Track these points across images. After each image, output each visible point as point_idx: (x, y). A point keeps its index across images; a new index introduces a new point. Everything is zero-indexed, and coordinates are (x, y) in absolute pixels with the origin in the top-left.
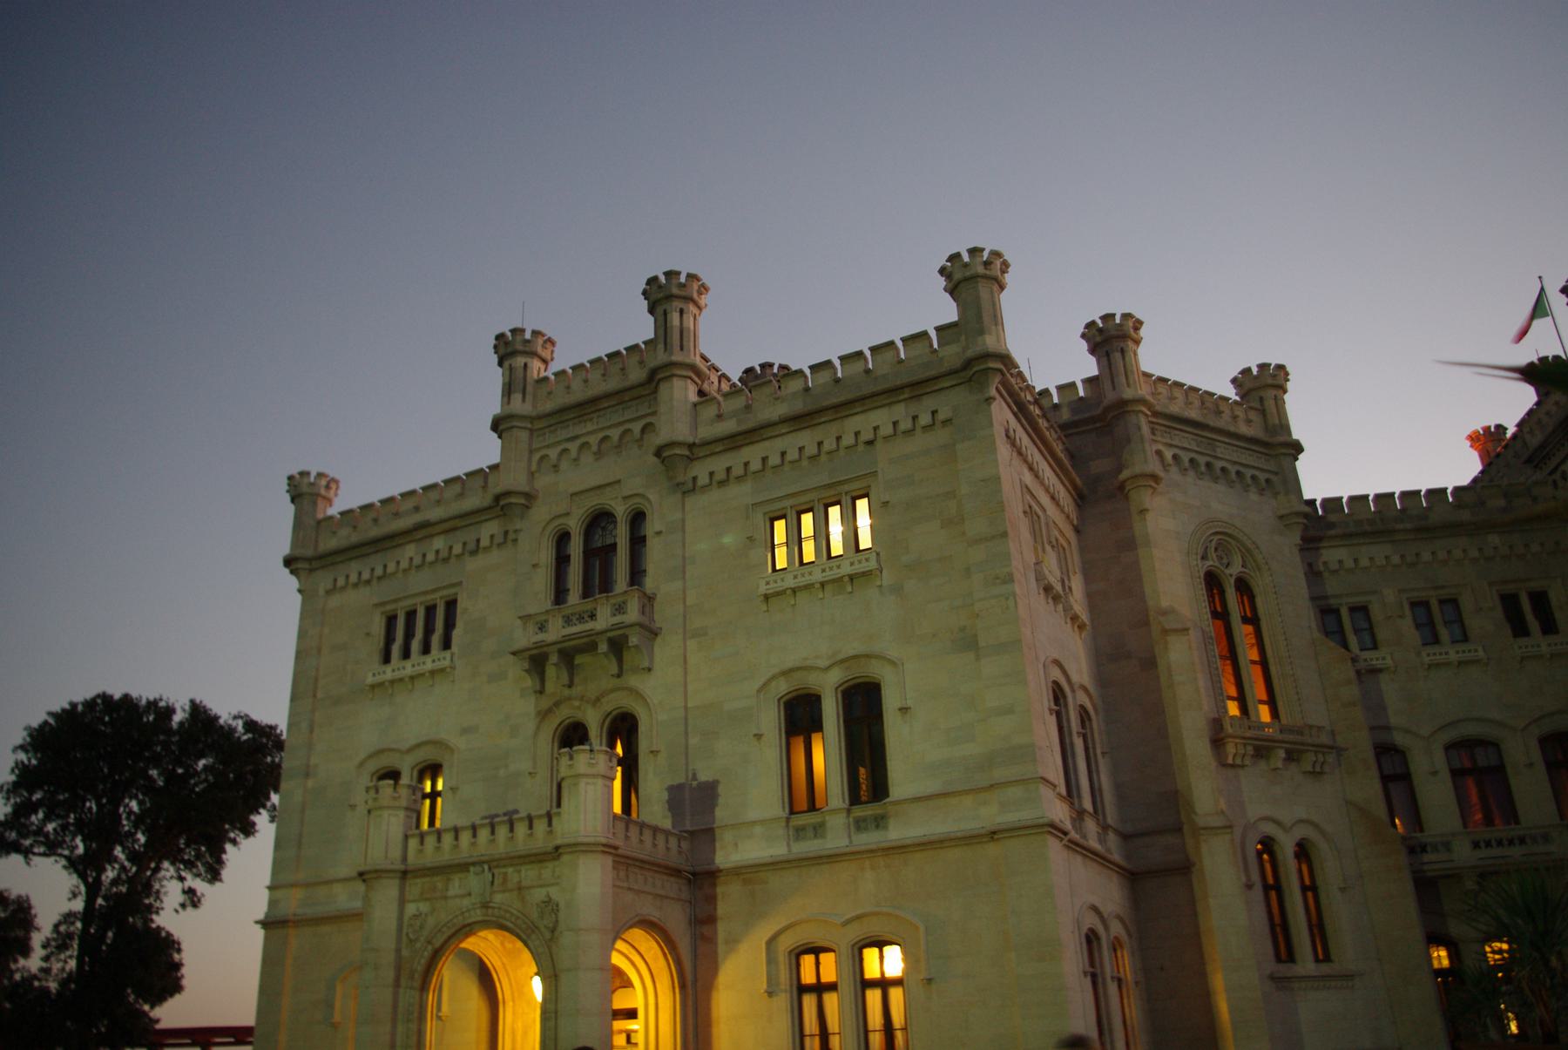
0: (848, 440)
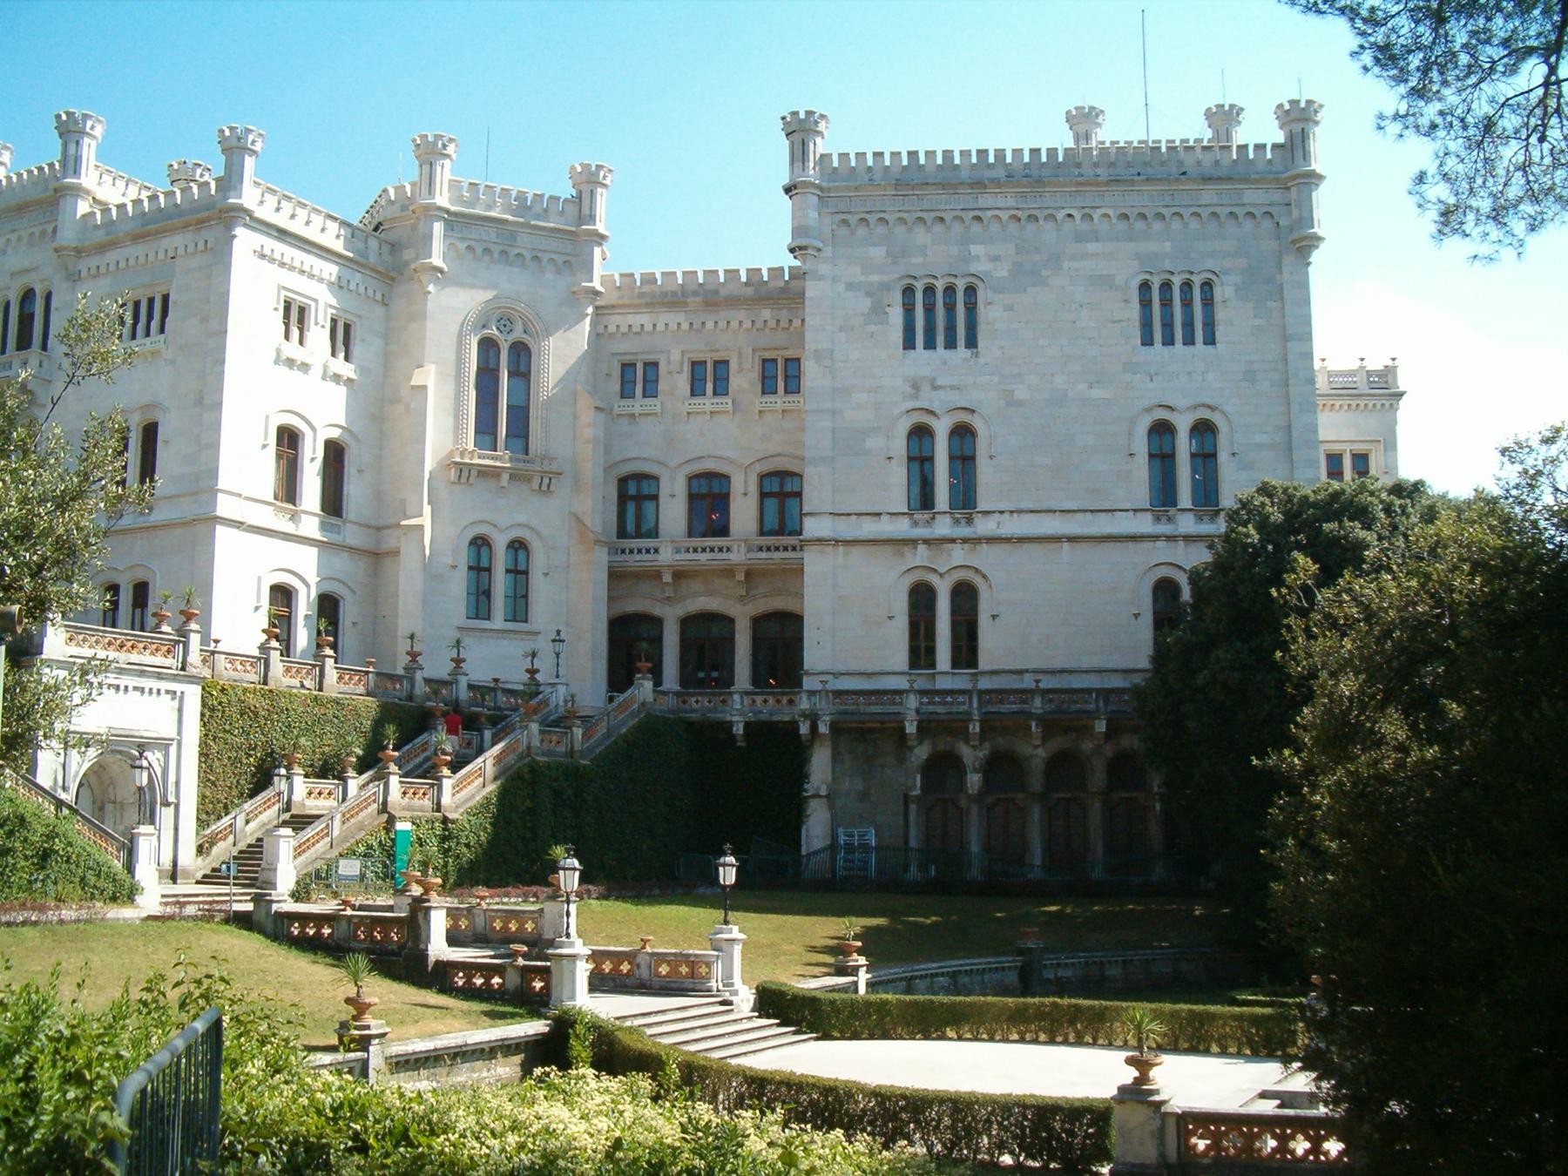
0: (161, 255)
